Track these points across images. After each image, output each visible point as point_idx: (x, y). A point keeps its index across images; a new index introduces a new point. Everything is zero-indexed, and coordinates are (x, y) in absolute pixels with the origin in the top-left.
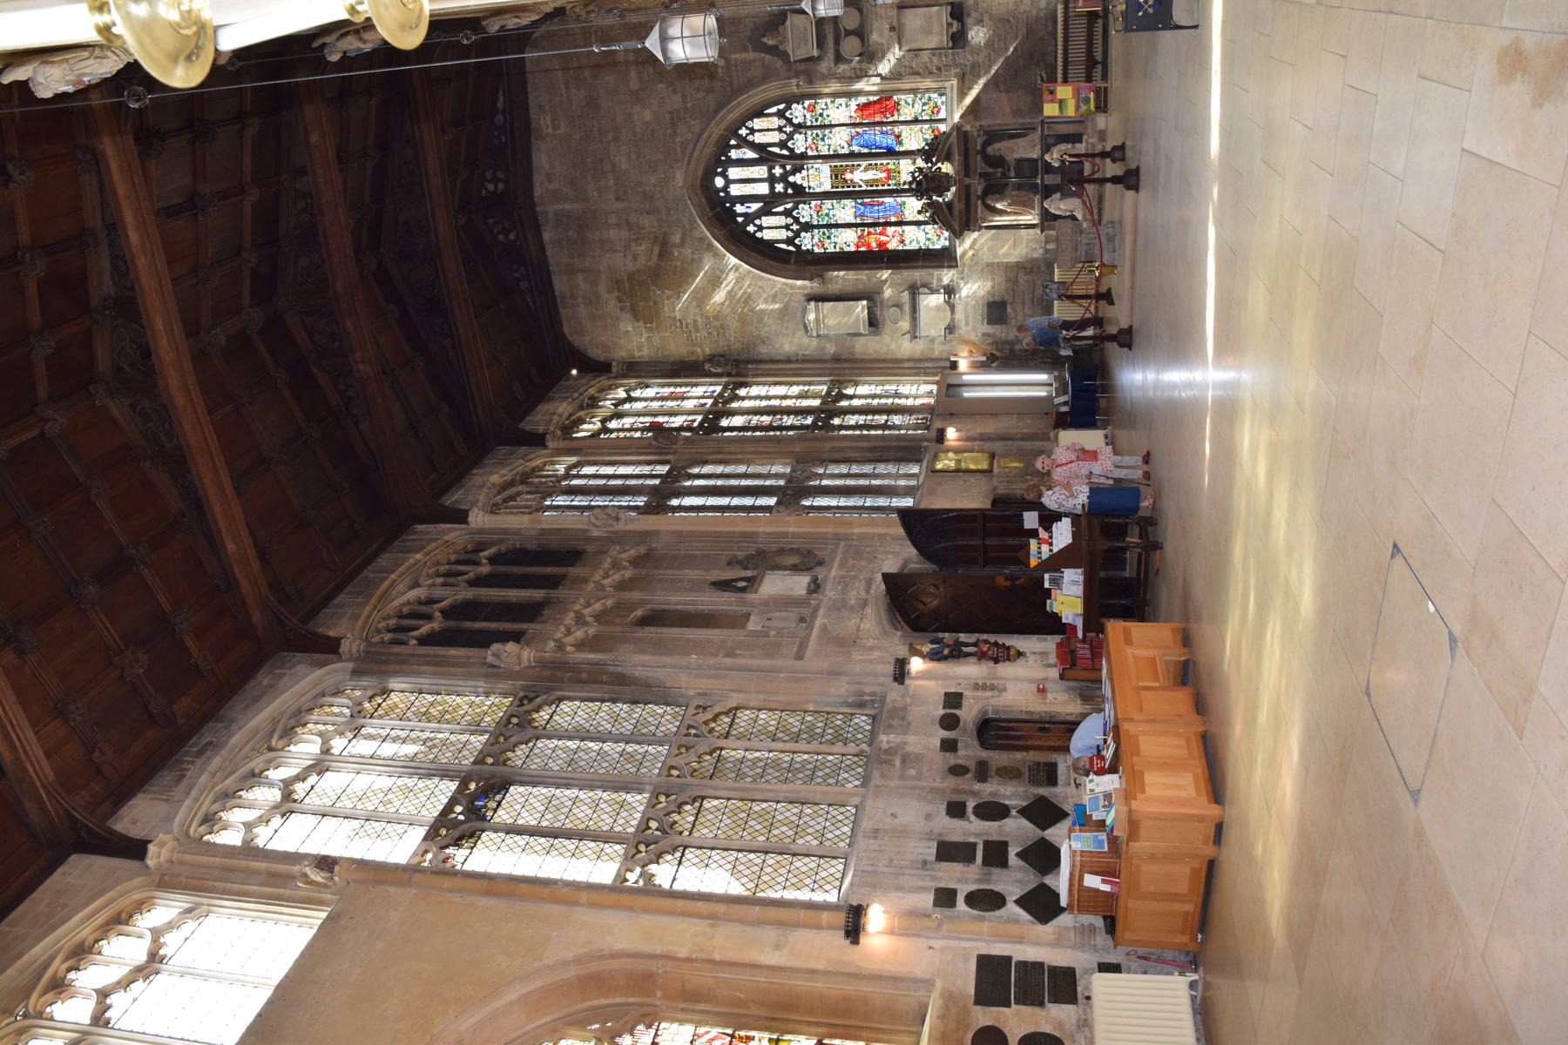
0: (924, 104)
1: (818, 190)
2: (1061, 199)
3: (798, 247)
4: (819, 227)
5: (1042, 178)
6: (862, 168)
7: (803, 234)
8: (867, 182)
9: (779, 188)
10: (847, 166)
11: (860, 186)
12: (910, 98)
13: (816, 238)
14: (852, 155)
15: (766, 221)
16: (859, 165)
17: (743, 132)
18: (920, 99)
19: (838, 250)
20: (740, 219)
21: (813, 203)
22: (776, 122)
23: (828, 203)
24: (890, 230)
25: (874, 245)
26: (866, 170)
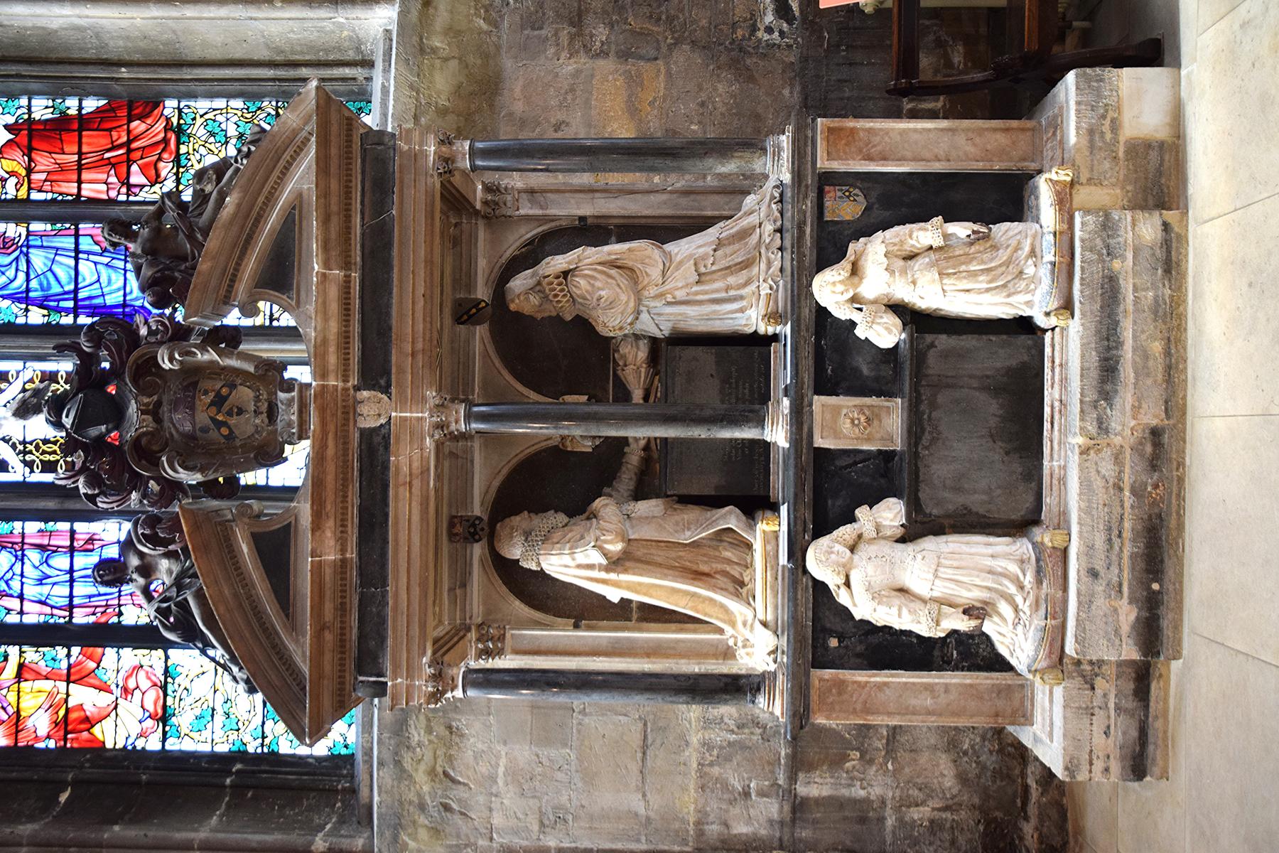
2: (908, 536)
5: (800, 418)
24: (115, 661)
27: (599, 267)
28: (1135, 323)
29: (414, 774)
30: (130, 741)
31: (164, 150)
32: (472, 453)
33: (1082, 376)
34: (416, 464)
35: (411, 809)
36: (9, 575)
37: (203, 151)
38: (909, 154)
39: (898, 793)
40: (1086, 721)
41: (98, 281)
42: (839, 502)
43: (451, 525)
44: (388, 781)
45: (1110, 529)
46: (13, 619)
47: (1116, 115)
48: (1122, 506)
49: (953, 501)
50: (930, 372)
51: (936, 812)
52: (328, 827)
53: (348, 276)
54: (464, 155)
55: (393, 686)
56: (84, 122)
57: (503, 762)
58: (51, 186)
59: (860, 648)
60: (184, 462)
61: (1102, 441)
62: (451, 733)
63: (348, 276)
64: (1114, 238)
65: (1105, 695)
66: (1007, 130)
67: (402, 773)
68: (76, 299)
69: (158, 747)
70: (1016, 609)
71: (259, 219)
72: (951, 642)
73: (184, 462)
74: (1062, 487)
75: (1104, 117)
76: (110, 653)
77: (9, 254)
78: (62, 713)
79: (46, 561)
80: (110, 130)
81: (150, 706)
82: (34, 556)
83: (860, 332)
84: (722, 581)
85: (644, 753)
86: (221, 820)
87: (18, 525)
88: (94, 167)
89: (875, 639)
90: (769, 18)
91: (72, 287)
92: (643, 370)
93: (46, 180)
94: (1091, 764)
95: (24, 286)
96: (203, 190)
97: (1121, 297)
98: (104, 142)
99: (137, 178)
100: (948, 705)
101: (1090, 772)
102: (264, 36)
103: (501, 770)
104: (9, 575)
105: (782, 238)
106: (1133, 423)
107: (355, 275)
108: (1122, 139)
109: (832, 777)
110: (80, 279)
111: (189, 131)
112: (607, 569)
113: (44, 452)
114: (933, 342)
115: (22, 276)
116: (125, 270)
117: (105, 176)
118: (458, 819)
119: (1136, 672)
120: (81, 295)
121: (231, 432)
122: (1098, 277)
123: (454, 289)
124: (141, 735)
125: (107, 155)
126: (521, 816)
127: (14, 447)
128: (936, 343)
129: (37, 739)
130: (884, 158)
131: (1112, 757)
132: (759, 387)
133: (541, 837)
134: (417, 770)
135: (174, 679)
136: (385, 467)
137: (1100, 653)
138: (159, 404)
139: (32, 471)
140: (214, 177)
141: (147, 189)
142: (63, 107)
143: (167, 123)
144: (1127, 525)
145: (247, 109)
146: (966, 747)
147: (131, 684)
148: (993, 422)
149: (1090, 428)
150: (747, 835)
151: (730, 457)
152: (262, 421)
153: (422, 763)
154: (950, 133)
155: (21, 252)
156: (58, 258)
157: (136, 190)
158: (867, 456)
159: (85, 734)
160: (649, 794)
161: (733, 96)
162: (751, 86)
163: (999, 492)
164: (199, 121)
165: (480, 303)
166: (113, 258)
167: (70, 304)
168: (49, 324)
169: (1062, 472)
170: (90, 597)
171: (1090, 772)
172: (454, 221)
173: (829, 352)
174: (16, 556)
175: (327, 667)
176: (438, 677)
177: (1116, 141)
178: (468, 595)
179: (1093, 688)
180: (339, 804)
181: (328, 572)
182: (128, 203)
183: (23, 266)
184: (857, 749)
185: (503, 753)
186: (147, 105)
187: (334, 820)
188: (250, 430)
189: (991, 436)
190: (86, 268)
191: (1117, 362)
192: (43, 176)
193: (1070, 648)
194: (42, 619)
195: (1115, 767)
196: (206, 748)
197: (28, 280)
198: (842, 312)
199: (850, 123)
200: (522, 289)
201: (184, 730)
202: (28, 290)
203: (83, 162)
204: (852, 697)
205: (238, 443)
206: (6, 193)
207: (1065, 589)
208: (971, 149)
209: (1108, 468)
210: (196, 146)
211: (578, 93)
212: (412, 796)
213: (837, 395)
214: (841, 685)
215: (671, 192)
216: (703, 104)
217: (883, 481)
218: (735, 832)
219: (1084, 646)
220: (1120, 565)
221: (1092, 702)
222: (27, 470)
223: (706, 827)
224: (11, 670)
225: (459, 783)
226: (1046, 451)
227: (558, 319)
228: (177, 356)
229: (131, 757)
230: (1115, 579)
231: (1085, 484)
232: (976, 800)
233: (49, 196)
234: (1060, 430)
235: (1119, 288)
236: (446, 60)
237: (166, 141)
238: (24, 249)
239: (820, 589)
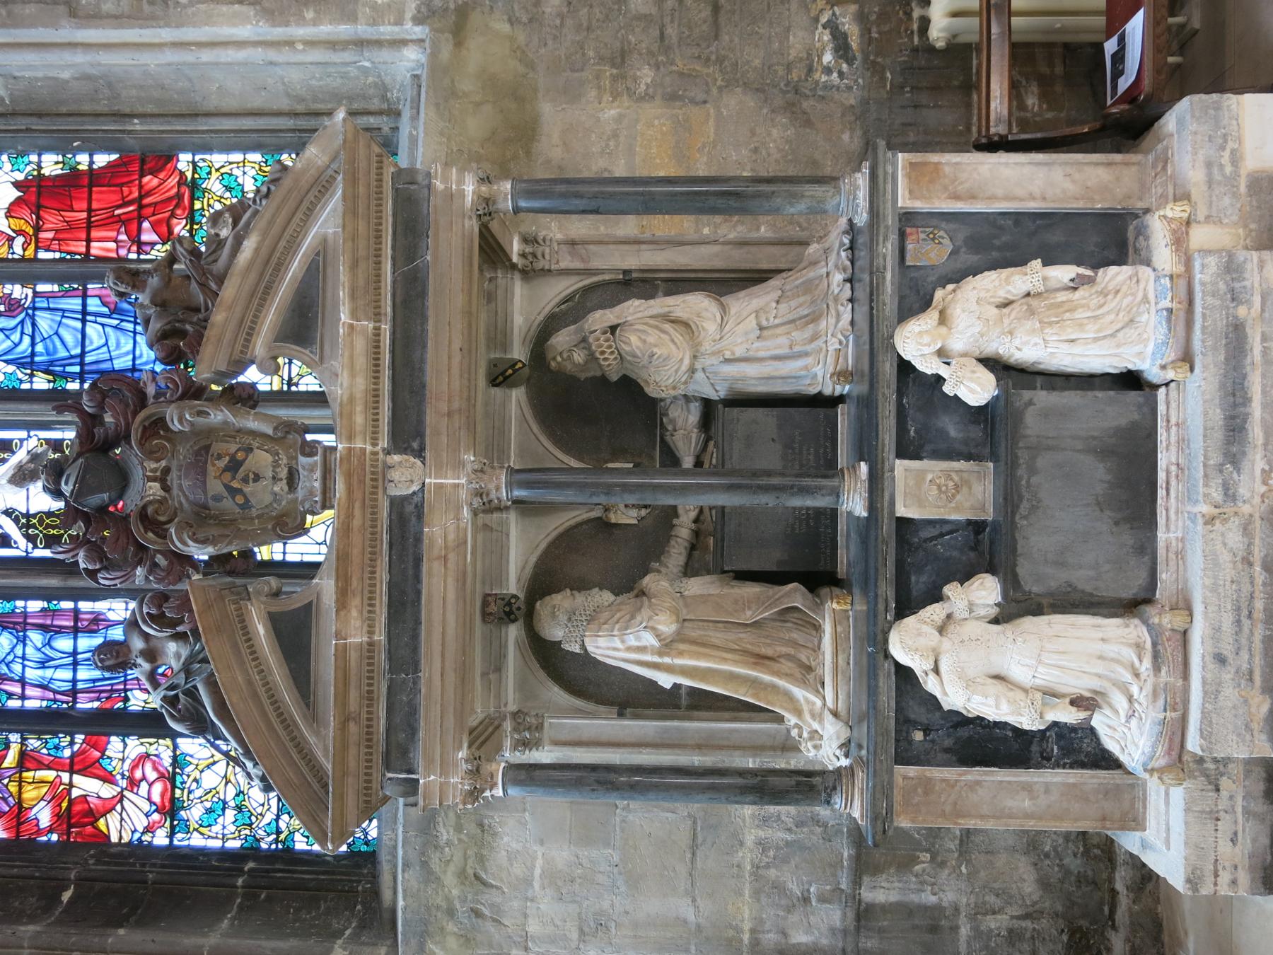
5: (877, 485)
25: (44, 815)
27: (652, 322)
28: (1264, 376)
29: (442, 877)
30: (137, 836)
31: (177, 206)
32: (508, 525)
33: (1205, 436)
34: (451, 537)
35: (439, 914)
36: (10, 658)
38: (1000, 192)
39: (972, 900)
40: (1210, 826)
41: (106, 344)
42: (924, 578)
43: (485, 603)
44: (414, 884)
45: (1238, 609)
46: (14, 704)
47: (1236, 146)
48: (1252, 583)
49: (1056, 579)
50: (1029, 432)
51: (1015, 921)
52: (348, 932)
53: (377, 329)
54: (506, 195)
55: (425, 783)
56: (95, 177)
57: (539, 863)
58: (59, 244)
59: (948, 743)
60: (194, 534)
61: (1229, 509)
62: (483, 831)
63: (377, 329)
64: (1239, 282)
65: (1231, 798)
66: (1109, 164)
67: (429, 876)
68: (82, 364)
69: (166, 842)
70: (1130, 699)
71: (280, 267)
72: (1051, 736)
73: (194, 534)
74: (1180, 562)
75: (1223, 148)
76: (115, 743)
77: (14, 317)
78: (64, 805)
79: (49, 644)
80: (122, 185)
81: (156, 798)
82: (36, 637)
83: (948, 389)
84: (787, 666)
85: (694, 854)
86: (232, 924)
87: (20, 603)
88: (104, 224)
89: (964, 733)
90: (828, 58)
91: (78, 351)
92: (694, 436)
93: (54, 239)
94: (1216, 875)
95: (30, 350)
96: (217, 235)
97: (1248, 347)
98: (115, 198)
99: (148, 236)
100: (1049, 806)
101: (1216, 884)
102: (284, 84)
103: (537, 872)
104: (10, 658)
105: (852, 289)
106: (1263, 489)
107: (386, 328)
108: (1243, 172)
109: (899, 881)
110: (87, 342)
111: (204, 186)
112: (661, 654)
113: (48, 526)
114: (1031, 399)
115: (27, 340)
116: (135, 333)
117: (113, 234)
118: (490, 927)
119: (1267, 772)
120: (88, 359)
121: (247, 500)
122: (1221, 324)
123: (488, 348)
124: (149, 829)
125: (117, 212)
126: (559, 923)
127: (16, 521)
128: (1035, 400)
129: (40, 832)
130: (973, 197)
131: (1239, 868)
132: (825, 453)
133: (581, 946)
134: (445, 872)
135: (182, 769)
136: (418, 540)
137: (1229, 750)
138: (167, 471)
139: (35, 547)
140: (230, 220)
141: (158, 247)
142: (72, 162)
143: (181, 178)
144: (1259, 605)
145: (266, 162)
146: (1047, 848)
148: (1100, 489)
149: (1215, 495)
150: (806, 944)
151: (793, 529)
152: (282, 489)
153: (452, 864)
154: (1046, 169)
155: (27, 314)
156: (64, 320)
157: (147, 248)
158: (955, 527)
159: (89, 829)
160: (699, 900)
161: (788, 141)
162: (808, 130)
163: (1107, 567)
164: (215, 175)
165: (516, 364)
166: (122, 320)
167: (77, 369)
168: (54, 389)
169: (1180, 545)
170: (94, 681)
171: (1216, 884)
172: (488, 276)
173: (911, 412)
174: (17, 638)
175: (352, 764)
176: (475, 773)
177: (1236, 174)
178: (503, 680)
179: (1218, 790)
180: (359, 907)
181: (353, 656)
182: (139, 261)
183: (29, 329)
184: (927, 851)
185: (540, 854)
186: (162, 160)
187: (353, 925)
188: (268, 499)
189: (1098, 504)
190: (93, 330)
191: (1245, 421)
192: (50, 235)
193: (1194, 743)
194: (44, 704)
195: (1244, 878)
196: (217, 844)
197: (33, 344)
198: (927, 365)
199: (934, 158)
200: (566, 346)
201: (193, 825)
202: (33, 354)
203: (93, 219)
204: (940, 797)
205: (254, 512)
206: (13, 253)
207: (1186, 675)
208: (1068, 185)
209: (1235, 539)
210: (211, 202)
211: (622, 139)
212: (439, 901)
213: (921, 459)
214: (927, 784)
215: (724, 244)
216: (756, 150)
217: (972, 554)
218: (794, 941)
219: (1210, 742)
220: (1250, 650)
221: (1216, 805)
222: (30, 546)
223: (761, 936)
224: (11, 759)
225: (492, 886)
226: (1161, 520)
227: (603, 380)
228: (187, 416)
229: (138, 851)
230: (1245, 666)
231: (1211, 560)
232: (1060, 908)
233: (57, 255)
234: (1177, 497)
235: (1246, 337)
236: (478, 104)
237: (179, 196)
238: (30, 312)
239: (904, 674)
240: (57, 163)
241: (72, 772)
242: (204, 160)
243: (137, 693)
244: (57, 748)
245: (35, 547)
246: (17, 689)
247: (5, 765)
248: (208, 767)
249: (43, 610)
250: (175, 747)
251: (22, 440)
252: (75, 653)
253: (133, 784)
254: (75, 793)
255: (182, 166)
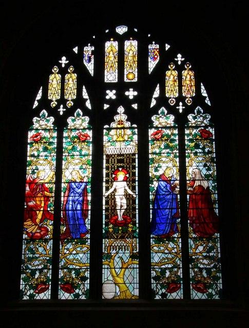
0: (209, 271)
1: (105, 138)
3: (36, 113)
4: (60, 138)
6: (130, 192)
7: (52, 119)
8: (112, 198)
9: (111, 95)
10: (134, 174)
11: (107, 189)
12: (217, 253)
13: (47, 135)
14: (145, 180)
15: (72, 80)
16: (133, 189)
17: (179, 58)
18: (215, 267)
19: (28, 159)
20: (76, 50)
21: (90, 133)
22: (189, 93)
23: (88, 149)
25: (31, 204)
26: (128, 197)
37: (204, 245)
41: (163, 215)
56: (212, 209)
68: (157, 209)
69: (24, 238)
81: (36, 234)
82: (81, 199)
87: (90, 194)
91: (161, 207)
93: (193, 199)
113: (111, 201)
115: (164, 193)
120: (158, 210)
124: (27, 232)
127: (113, 192)
129: (27, 203)
147: (43, 229)
167: (156, 208)
170: (69, 215)
174: (81, 194)
192: (194, 198)
194: (62, 202)
196: (23, 253)
229: (21, 230)
240: (215, 198)
241: (43, 211)
242: (218, 241)
243: (65, 228)
244: (50, 206)
245: (106, 198)
246: (66, 195)
247: (46, 192)
248: (44, 249)
249: (88, 201)
250: (50, 240)
251: (135, 193)
252: (76, 210)
253: (40, 228)
254: (38, 212)
255: (216, 234)
